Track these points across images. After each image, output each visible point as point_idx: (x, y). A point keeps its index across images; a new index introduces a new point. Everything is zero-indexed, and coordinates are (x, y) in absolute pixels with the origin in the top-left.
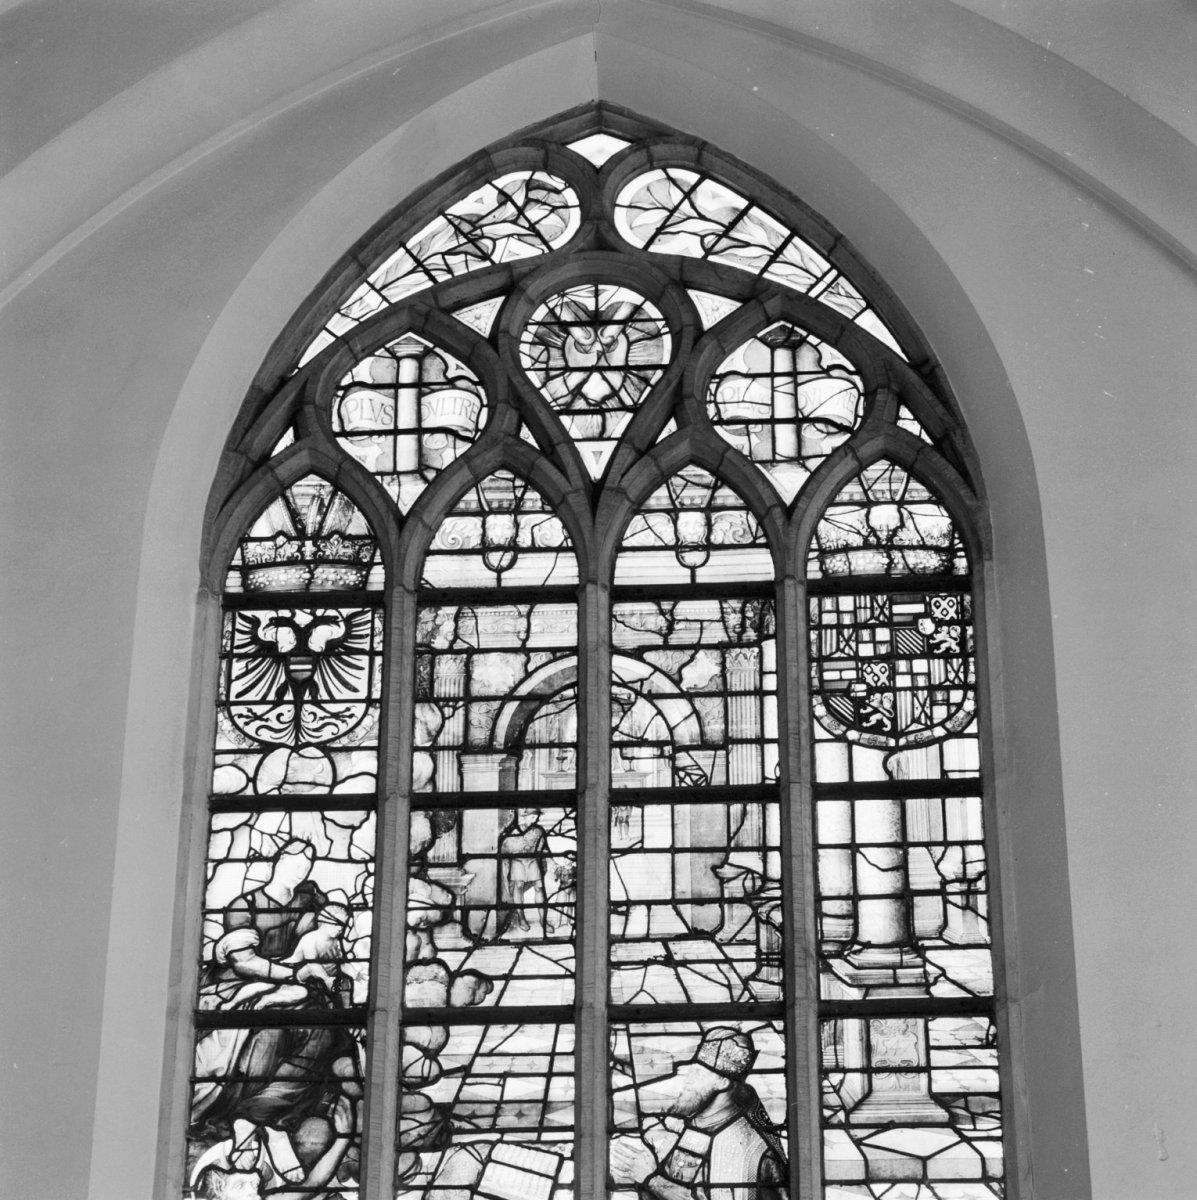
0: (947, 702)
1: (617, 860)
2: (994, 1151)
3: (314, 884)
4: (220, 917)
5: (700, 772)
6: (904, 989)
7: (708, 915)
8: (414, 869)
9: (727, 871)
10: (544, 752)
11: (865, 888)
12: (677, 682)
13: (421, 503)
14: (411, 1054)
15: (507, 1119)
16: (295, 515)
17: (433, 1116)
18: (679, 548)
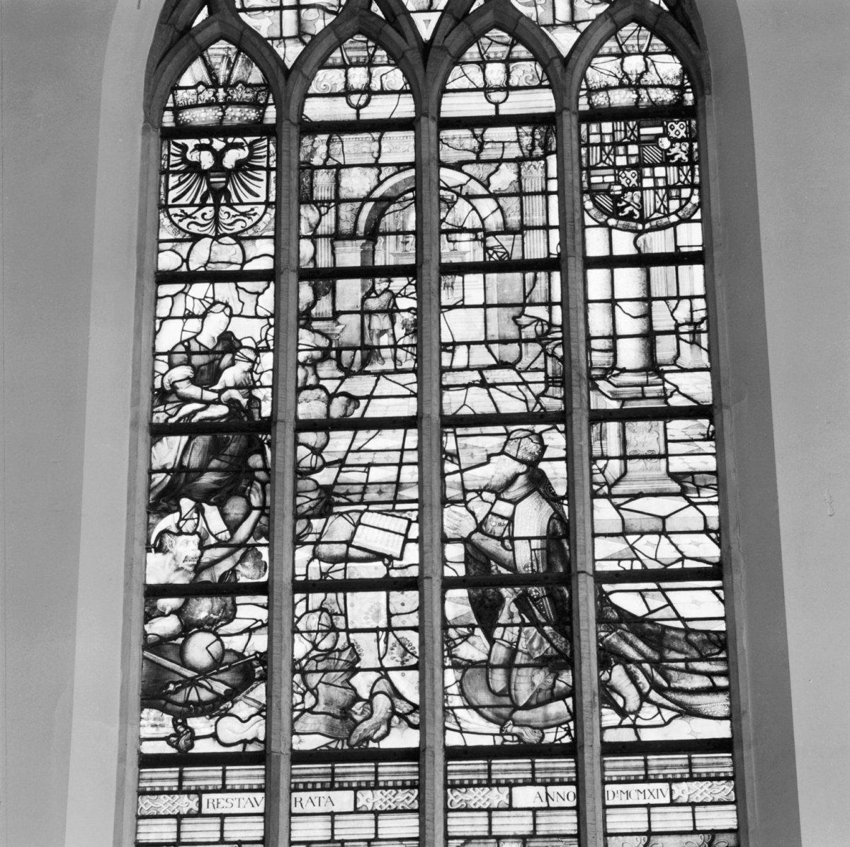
0: (679, 197)
1: (445, 314)
2: (713, 512)
3: (231, 333)
4: (165, 358)
5: (504, 251)
6: (649, 401)
7: (510, 352)
8: (302, 322)
9: (524, 320)
10: (393, 238)
11: (621, 330)
12: (487, 186)
13: (301, 59)
14: (302, 451)
15: (371, 495)
16: (210, 70)
17: (319, 494)
18: (486, 89)
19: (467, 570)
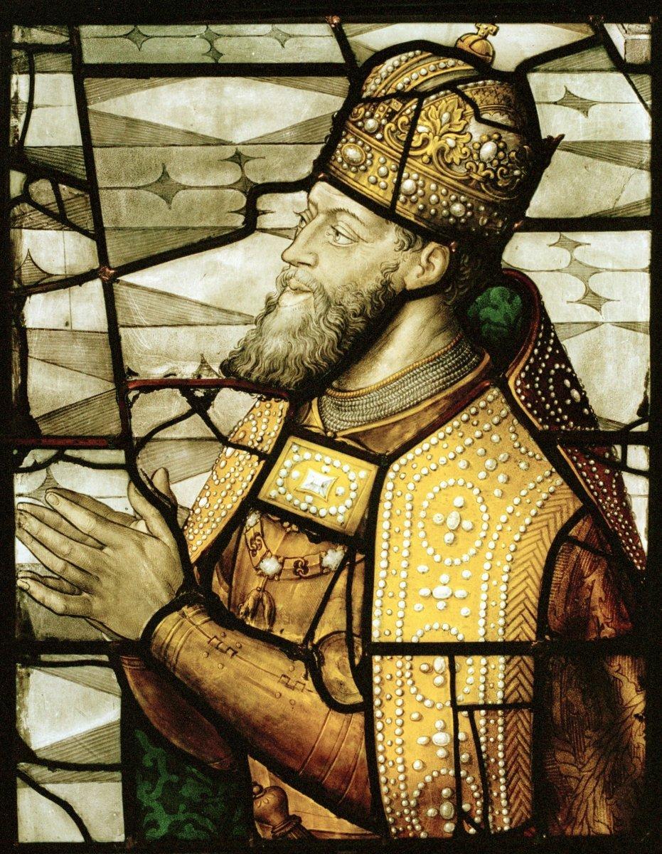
19: (133, 811)
